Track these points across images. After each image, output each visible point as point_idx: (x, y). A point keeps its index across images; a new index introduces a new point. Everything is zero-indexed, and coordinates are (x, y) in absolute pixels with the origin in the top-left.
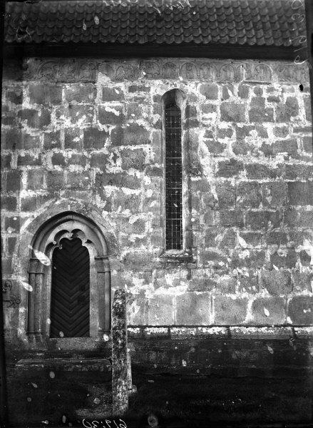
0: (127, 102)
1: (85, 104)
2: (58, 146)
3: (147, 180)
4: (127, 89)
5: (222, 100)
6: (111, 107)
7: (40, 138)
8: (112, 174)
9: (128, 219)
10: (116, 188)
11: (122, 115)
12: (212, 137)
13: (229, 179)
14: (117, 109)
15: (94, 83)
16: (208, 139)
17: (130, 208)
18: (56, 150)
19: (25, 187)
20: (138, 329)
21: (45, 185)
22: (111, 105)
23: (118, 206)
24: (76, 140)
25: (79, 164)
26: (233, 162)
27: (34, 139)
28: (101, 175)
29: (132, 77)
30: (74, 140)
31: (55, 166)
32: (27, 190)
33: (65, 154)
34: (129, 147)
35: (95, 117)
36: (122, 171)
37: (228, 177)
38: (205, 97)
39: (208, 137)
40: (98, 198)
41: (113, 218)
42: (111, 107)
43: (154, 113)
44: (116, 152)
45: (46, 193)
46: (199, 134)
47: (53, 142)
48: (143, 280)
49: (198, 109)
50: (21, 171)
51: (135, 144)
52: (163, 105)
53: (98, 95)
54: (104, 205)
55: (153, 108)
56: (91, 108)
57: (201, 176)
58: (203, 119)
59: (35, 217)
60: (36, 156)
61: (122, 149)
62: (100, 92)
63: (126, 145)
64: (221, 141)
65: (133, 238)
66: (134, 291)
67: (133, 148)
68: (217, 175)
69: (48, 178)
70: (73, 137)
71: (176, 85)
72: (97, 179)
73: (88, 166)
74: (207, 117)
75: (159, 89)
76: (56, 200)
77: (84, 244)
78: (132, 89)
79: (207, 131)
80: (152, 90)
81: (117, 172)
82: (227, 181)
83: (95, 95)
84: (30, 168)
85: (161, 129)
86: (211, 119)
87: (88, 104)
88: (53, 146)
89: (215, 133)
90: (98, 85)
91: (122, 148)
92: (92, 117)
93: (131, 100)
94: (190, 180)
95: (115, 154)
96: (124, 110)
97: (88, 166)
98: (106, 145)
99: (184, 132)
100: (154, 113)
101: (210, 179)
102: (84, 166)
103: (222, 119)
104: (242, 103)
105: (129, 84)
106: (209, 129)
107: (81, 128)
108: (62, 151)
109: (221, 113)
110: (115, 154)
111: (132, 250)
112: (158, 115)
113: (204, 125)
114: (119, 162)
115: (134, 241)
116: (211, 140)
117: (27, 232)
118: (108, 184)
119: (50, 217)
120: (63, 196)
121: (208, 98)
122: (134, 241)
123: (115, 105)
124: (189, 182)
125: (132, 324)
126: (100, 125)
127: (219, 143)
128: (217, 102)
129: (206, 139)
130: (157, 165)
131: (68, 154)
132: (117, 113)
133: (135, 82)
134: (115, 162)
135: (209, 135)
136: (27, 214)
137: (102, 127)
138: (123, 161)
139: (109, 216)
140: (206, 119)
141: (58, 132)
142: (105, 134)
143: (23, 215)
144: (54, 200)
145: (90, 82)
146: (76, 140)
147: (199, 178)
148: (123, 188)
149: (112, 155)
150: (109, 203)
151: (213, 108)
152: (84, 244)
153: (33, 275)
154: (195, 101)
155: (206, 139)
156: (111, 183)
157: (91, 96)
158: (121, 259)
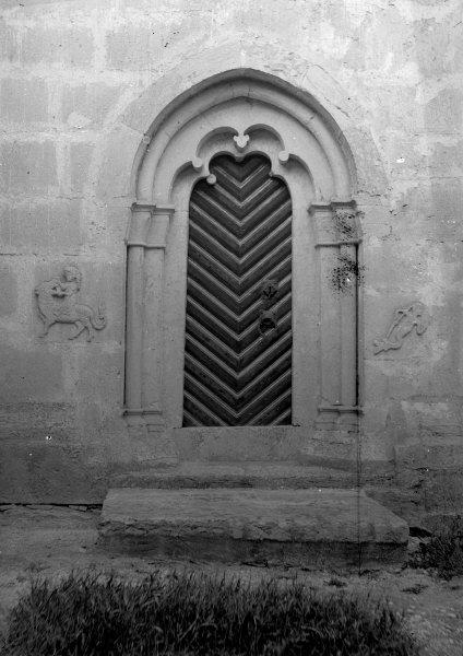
40: (327, 32)
59: (147, 82)
76: (206, 37)
143: (116, 78)
152: (276, 170)
153: (137, 253)
158: (393, 204)
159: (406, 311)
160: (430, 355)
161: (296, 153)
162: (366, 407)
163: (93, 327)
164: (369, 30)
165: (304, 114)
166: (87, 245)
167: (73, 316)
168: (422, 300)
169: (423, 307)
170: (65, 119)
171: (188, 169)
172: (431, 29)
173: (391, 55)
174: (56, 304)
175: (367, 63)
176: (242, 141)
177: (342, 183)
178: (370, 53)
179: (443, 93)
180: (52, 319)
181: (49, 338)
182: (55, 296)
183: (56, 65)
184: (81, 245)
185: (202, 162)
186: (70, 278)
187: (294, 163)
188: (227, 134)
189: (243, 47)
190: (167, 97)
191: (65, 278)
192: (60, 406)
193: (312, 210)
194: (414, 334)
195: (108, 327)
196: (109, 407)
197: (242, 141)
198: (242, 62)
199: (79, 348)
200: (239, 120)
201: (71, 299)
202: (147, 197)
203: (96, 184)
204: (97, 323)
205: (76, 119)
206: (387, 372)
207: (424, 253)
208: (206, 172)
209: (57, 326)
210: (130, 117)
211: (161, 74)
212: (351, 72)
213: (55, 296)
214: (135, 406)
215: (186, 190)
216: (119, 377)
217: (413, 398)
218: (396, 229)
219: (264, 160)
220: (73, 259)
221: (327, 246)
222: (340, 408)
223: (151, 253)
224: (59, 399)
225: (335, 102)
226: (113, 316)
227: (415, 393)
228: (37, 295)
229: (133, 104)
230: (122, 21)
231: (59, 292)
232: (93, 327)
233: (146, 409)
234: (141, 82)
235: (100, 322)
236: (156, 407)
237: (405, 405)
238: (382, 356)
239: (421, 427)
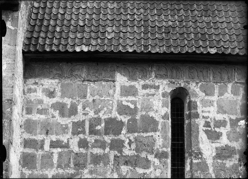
0: (140, 98)
1: (106, 99)
2: (84, 132)
3: (157, 161)
4: (141, 87)
5: (218, 97)
6: (128, 101)
7: (69, 126)
8: (127, 156)
10: (131, 168)
11: (136, 107)
12: (210, 127)
13: (224, 162)
14: (132, 102)
15: (114, 81)
16: (207, 129)
18: (81, 136)
19: (56, 166)
21: (72, 165)
22: (127, 99)
24: (99, 128)
25: (100, 147)
26: (227, 148)
27: (64, 126)
28: (118, 157)
29: (144, 77)
30: (97, 128)
31: (81, 149)
33: (88, 140)
34: (142, 134)
35: (114, 109)
36: (136, 154)
37: (223, 160)
38: (204, 94)
39: (207, 127)
42: (128, 101)
43: (163, 107)
44: (132, 138)
46: (201, 122)
47: (79, 129)
49: (198, 103)
50: (52, 153)
51: (147, 131)
52: (169, 100)
53: (117, 91)
55: (161, 102)
56: (111, 102)
57: (201, 158)
58: (202, 111)
60: (66, 141)
61: (136, 136)
62: (118, 89)
63: (140, 132)
64: (217, 130)
67: (145, 135)
68: (214, 158)
69: (75, 159)
70: (96, 126)
71: (180, 84)
72: (115, 160)
73: (107, 150)
74: (206, 110)
75: (166, 87)
78: (145, 87)
79: (206, 122)
80: (161, 88)
81: (132, 155)
82: (223, 163)
83: (114, 91)
84: (59, 150)
85: (168, 119)
86: (209, 112)
87: (109, 98)
88: (79, 133)
89: (212, 124)
90: (117, 84)
91: (136, 134)
92: (112, 110)
93: (144, 96)
94: (191, 161)
95: (130, 140)
96: (138, 104)
97: (107, 150)
98: (123, 132)
99: (187, 122)
100: (163, 107)
101: (210, 162)
102: (104, 149)
103: (218, 112)
104: (235, 99)
105: (142, 82)
106: (209, 120)
107: (103, 118)
108: (86, 137)
109: (218, 107)
110: (130, 140)
112: (166, 109)
113: (203, 117)
114: (133, 146)
116: (209, 129)
118: (124, 164)
121: (207, 95)
123: (131, 99)
124: (191, 163)
126: (118, 115)
127: (215, 131)
128: (215, 98)
129: (205, 129)
130: (165, 149)
131: (91, 139)
132: (132, 106)
133: (147, 81)
134: (130, 146)
135: (207, 124)
137: (120, 118)
138: (137, 146)
140: (205, 112)
141: (84, 121)
142: (122, 123)
145: (111, 81)
146: (99, 128)
147: (200, 161)
148: (137, 168)
149: (127, 141)
151: (211, 103)
154: (196, 97)
155: (205, 129)
156: (126, 163)
157: (111, 92)
172: (146, 176)
230: (57, 172)
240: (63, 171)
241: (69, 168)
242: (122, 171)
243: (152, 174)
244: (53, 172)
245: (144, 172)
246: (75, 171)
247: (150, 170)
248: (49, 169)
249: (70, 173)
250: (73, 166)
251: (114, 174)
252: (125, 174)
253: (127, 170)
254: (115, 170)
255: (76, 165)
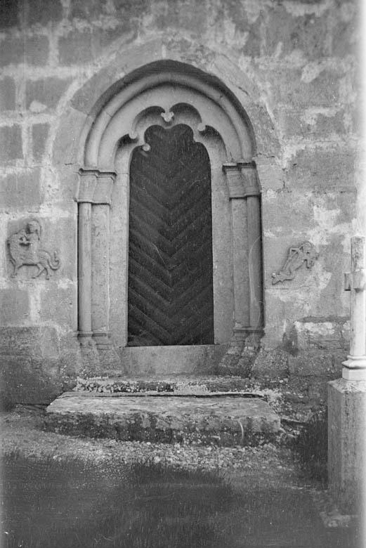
9: (299, 73)
17: (301, 47)
19: (68, 12)
20: (329, 325)
23: (274, 44)
32: (70, 19)
40: (229, 27)
41: (263, 72)
45: (112, 23)
48: (336, 212)
54: (242, 40)
59: (90, 74)
65: (310, 116)
66: (316, 238)
76: (135, 37)
77: (197, 139)
111: (310, 145)
115: (313, 123)
117: (73, 110)
119: (122, 75)
120: (150, 27)
122: (313, 123)
125: (314, 314)
136: (74, 71)
139: (256, 66)
143: (63, 72)
144: (130, 36)
150: (254, 35)
153: (87, 207)
158: (285, 165)
159: (297, 249)
160: (318, 285)
161: (211, 125)
162: (266, 329)
163: (51, 268)
164: (262, 25)
165: (215, 94)
166: (45, 203)
167: (36, 261)
168: (310, 241)
169: (312, 246)
170: (28, 107)
171: (125, 141)
172: (312, 22)
173: (280, 44)
174: (22, 250)
175: (262, 51)
176: (168, 116)
177: (246, 148)
178: (264, 42)
179: (323, 73)
180: (21, 262)
181: (18, 278)
182: (22, 245)
183: (21, 66)
184: (40, 204)
185: (139, 134)
186: (32, 229)
187: (210, 132)
188: (155, 111)
189: (163, 43)
190: (105, 84)
191: (28, 231)
192: (28, 330)
193: (224, 168)
194: (304, 266)
195: (62, 267)
196: (63, 330)
197: (168, 116)
198: (164, 55)
199: (41, 286)
200: (165, 100)
201: (35, 245)
202: (93, 160)
203: (51, 156)
204: (53, 264)
205: (36, 106)
206: (281, 298)
207: (311, 203)
208: (142, 141)
209: (24, 268)
210: (77, 102)
211: (100, 67)
212: (249, 59)
213: (22, 245)
214: (87, 328)
215: (125, 158)
216: (71, 306)
217: (304, 321)
218: (288, 183)
219: (188, 130)
220: (36, 215)
221: (237, 198)
222: (249, 329)
223: (97, 208)
224: (27, 324)
225: (238, 83)
226: (66, 258)
227: (306, 316)
228: (8, 245)
229: (79, 92)
230: (71, 29)
231: (25, 241)
232: (51, 268)
233: (96, 332)
234: (84, 75)
235: (56, 263)
236: (105, 330)
237: (298, 325)
238: (279, 286)
239: (309, 342)
240: (86, 25)
241: (101, 16)
242: (245, 13)
243: (330, 17)
244: (62, 28)
245: (307, 12)
246: (118, 22)
247: (323, 7)
248: (50, 23)
249: (105, 27)
250: (113, 8)
251: (225, 22)
252: (254, 20)
253: (259, 8)
254: (226, 12)
255: (122, 6)
